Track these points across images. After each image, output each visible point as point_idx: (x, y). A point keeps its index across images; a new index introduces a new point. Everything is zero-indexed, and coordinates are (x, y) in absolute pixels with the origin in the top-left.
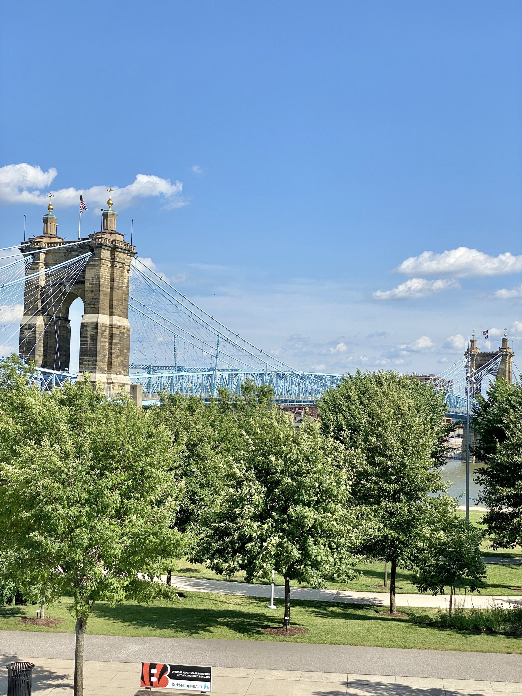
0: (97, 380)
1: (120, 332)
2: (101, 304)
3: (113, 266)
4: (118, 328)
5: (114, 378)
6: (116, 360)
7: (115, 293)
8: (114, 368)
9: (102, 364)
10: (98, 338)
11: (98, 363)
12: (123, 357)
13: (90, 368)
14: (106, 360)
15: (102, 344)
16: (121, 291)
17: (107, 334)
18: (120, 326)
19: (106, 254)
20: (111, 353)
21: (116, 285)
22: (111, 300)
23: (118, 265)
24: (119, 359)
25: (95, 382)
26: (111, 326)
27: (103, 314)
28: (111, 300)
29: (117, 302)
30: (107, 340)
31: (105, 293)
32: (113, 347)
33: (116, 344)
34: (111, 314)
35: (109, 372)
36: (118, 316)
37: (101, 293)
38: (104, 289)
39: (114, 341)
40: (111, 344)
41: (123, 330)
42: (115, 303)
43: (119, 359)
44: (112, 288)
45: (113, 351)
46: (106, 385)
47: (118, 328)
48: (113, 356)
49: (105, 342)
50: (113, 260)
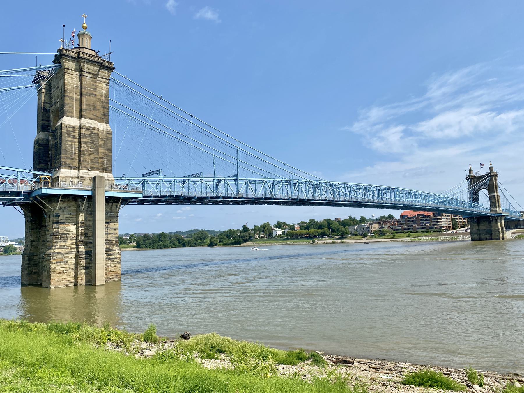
0: (60, 175)
1: (91, 133)
2: (67, 108)
3: (81, 76)
4: (89, 129)
5: (83, 173)
6: (86, 157)
7: (84, 99)
8: (83, 164)
9: (70, 160)
10: (63, 138)
11: (62, 160)
12: (98, 155)
13: (59, 165)
14: (77, 157)
15: (69, 143)
16: (92, 98)
17: (76, 134)
18: (91, 127)
19: (70, 65)
20: (80, 151)
21: (85, 91)
22: (81, 105)
23: (87, 75)
24: (92, 157)
25: (59, 177)
26: (80, 127)
27: (71, 117)
28: (81, 105)
29: (88, 107)
30: (77, 140)
31: (72, 99)
32: (82, 145)
33: (85, 143)
34: (81, 117)
35: (79, 168)
36: (90, 119)
37: (66, 98)
38: (71, 95)
39: (82, 140)
40: (80, 143)
41: (96, 132)
42: (84, 107)
43: (92, 157)
44: (81, 95)
45: (82, 149)
46: (75, 180)
47: (89, 129)
48: (82, 153)
49: (72, 141)
50: (80, 71)
